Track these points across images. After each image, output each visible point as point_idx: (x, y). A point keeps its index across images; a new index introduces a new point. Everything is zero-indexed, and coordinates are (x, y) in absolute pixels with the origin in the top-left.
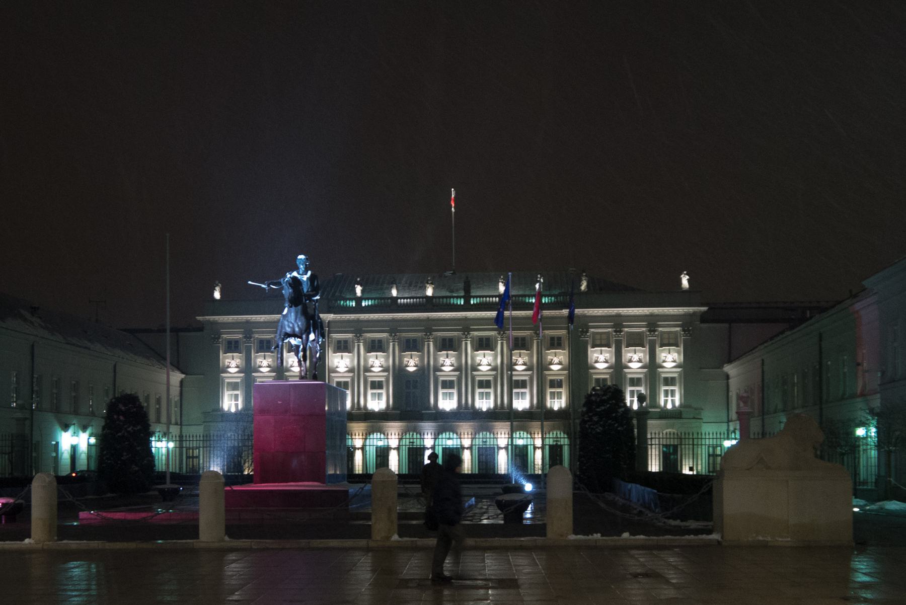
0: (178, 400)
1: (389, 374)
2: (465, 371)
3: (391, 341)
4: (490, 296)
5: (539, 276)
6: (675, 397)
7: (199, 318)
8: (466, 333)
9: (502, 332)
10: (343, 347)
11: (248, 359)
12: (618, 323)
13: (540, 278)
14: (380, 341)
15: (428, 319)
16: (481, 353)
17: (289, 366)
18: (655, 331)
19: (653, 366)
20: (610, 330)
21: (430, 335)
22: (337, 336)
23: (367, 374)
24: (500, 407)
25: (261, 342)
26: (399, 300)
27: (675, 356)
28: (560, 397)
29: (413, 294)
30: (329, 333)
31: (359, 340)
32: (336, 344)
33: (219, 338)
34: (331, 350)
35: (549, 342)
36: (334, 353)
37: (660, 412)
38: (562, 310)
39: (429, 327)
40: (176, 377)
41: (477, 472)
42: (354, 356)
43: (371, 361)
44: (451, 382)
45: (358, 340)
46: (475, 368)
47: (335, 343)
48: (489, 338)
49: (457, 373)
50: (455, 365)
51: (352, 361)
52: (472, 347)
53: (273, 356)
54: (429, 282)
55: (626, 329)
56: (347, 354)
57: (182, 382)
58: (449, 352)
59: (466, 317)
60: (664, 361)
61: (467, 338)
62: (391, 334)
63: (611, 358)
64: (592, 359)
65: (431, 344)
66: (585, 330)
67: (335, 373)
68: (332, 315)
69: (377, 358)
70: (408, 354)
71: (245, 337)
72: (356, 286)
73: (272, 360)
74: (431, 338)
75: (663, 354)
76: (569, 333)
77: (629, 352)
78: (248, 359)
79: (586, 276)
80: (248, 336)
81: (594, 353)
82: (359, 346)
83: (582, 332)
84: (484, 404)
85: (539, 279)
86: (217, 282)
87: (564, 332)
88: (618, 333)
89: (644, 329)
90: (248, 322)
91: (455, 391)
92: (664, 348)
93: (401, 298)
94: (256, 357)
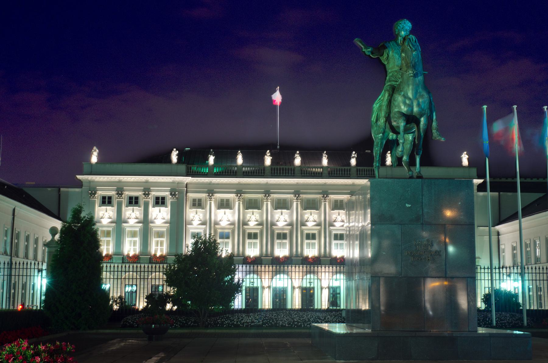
3: (237, 200)
7: (79, 177)
10: (198, 204)
11: (119, 212)
13: (355, 154)
14: (228, 201)
17: (153, 218)
26: (244, 169)
30: (187, 193)
31: (212, 198)
33: (95, 193)
42: (206, 211)
43: (248, 216)
45: (210, 199)
47: (191, 201)
50: (288, 221)
51: (205, 215)
52: (302, 207)
53: (140, 210)
56: (200, 210)
61: (298, 199)
65: (269, 203)
68: (190, 178)
69: (311, 215)
70: (251, 211)
71: (117, 194)
72: (209, 155)
73: (140, 213)
74: (269, 199)
78: (119, 212)
80: (120, 192)
84: (311, 252)
86: (95, 148)
90: (120, 182)
91: (287, 241)
94: (126, 211)
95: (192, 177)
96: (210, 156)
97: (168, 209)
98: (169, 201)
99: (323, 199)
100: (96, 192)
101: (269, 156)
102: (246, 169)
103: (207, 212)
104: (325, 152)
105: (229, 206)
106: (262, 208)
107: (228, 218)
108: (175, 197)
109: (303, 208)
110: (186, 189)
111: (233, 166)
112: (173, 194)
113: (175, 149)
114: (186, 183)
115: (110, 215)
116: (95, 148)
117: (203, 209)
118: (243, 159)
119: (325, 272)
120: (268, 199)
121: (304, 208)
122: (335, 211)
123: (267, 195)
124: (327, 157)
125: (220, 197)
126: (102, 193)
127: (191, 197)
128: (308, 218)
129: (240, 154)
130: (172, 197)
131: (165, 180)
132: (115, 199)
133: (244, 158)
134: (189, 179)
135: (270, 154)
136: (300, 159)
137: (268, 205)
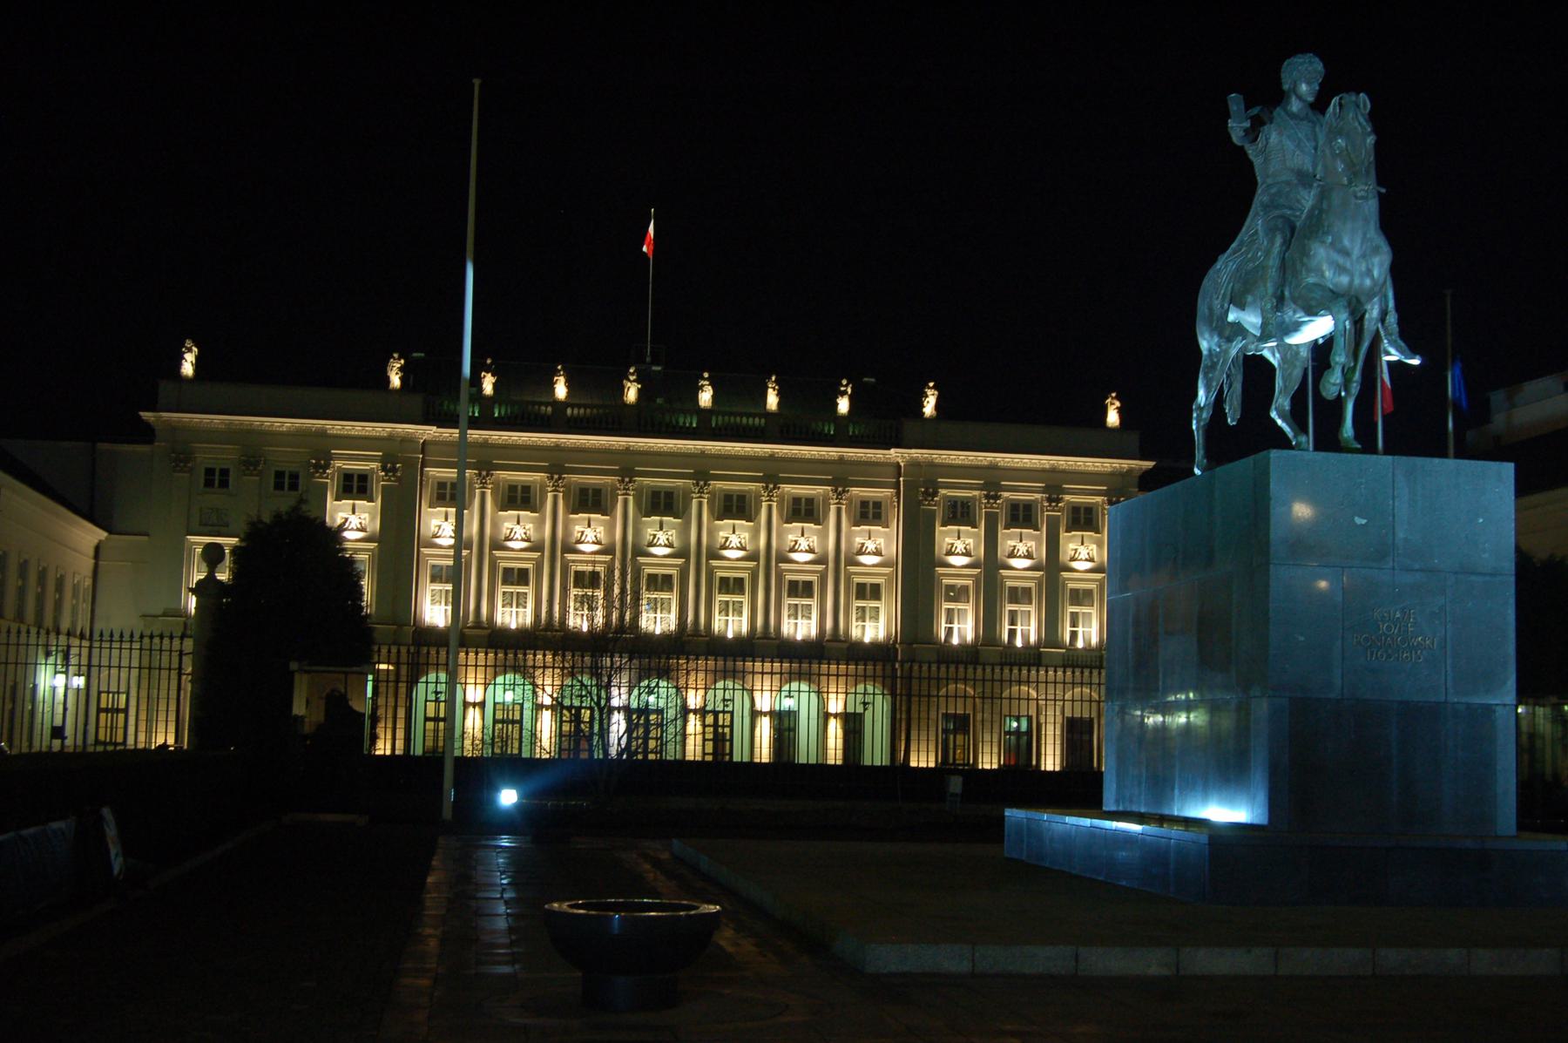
0: (88, 586)
1: (543, 556)
2: (770, 561)
4: (741, 415)
5: (844, 382)
6: (1078, 627)
7: (146, 415)
8: (702, 483)
9: (771, 486)
12: (992, 481)
13: (847, 386)
14: (526, 489)
15: (627, 451)
16: (796, 527)
18: (1058, 500)
19: (1053, 566)
20: (976, 493)
21: (630, 482)
22: (439, 472)
23: (498, 553)
24: (761, 633)
25: (348, 477)
26: (569, 411)
27: (1092, 550)
28: (876, 618)
29: (589, 401)
31: (486, 483)
32: (436, 487)
34: (425, 502)
35: (859, 510)
36: (430, 507)
37: (1063, 654)
38: (889, 449)
39: (627, 466)
40: (88, 536)
41: (839, 762)
44: (667, 579)
46: (714, 555)
47: (432, 488)
48: (672, 493)
49: (680, 561)
54: (632, 378)
55: (1006, 494)
57: (97, 549)
58: (665, 518)
59: (703, 452)
60: (1073, 559)
61: (703, 492)
62: (552, 474)
63: (977, 546)
64: (941, 548)
66: (931, 490)
67: (648, 556)
68: (434, 428)
70: (584, 519)
74: (631, 488)
75: (1072, 546)
76: (898, 494)
77: (1010, 537)
79: (934, 387)
81: (1070, 542)
82: (483, 495)
83: (926, 493)
85: (842, 389)
86: (188, 343)
87: (888, 492)
88: (991, 501)
89: (1038, 496)
92: (1073, 533)
93: (573, 406)
95: (438, 427)
96: (485, 376)
97: (375, 507)
98: (377, 489)
99: (766, 494)
100: (330, 464)
101: (634, 381)
102: (576, 411)
103: (690, 527)
104: (773, 378)
105: (672, 508)
106: (611, 512)
107: (525, 533)
108: (394, 476)
109: (782, 519)
110: (421, 456)
111: (541, 404)
112: (388, 465)
113: (396, 355)
114: (422, 441)
115: (363, 522)
116: (188, 343)
117: (817, 523)
118: (568, 387)
119: (828, 675)
120: (628, 489)
121: (716, 514)
122: (794, 524)
123: (627, 480)
124: (778, 390)
125: (507, 481)
126: (344, 467)
127: (434, 477)
128: (727, 539)
129: (562, 373)
130: (386, 475)
131: (369, 431)
132: (378, 482)
133: (569, 384)
134: (430, 432)
135: (637, 376)
136: (712, 392)
137: (624, 504)
